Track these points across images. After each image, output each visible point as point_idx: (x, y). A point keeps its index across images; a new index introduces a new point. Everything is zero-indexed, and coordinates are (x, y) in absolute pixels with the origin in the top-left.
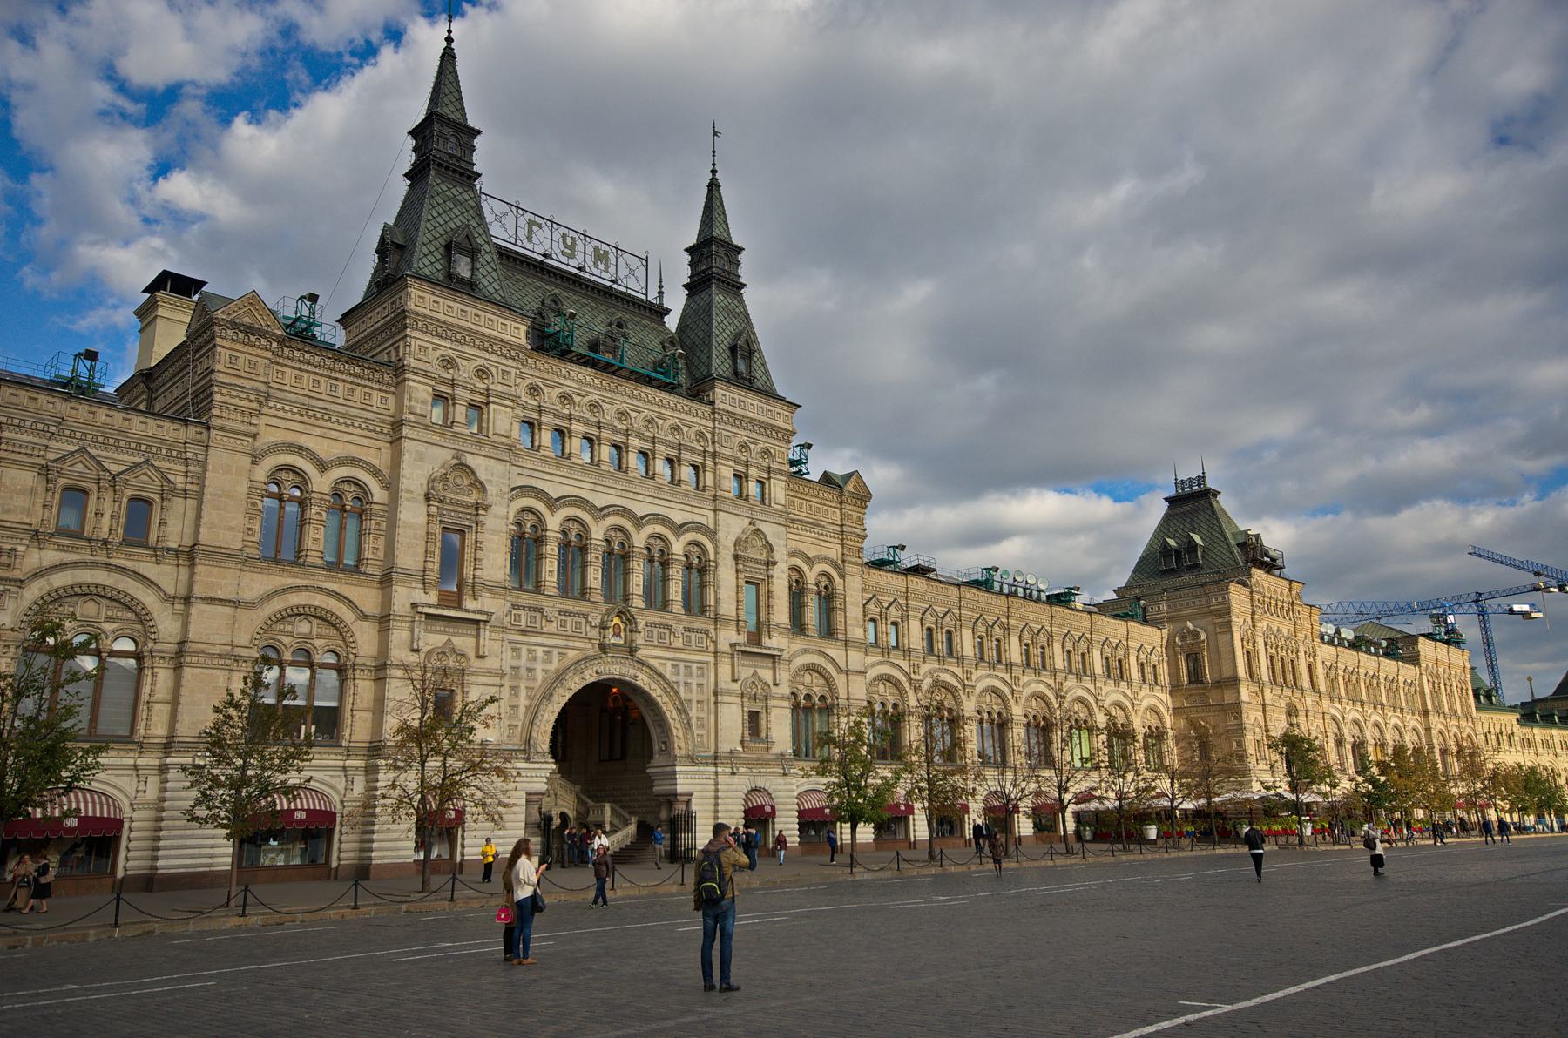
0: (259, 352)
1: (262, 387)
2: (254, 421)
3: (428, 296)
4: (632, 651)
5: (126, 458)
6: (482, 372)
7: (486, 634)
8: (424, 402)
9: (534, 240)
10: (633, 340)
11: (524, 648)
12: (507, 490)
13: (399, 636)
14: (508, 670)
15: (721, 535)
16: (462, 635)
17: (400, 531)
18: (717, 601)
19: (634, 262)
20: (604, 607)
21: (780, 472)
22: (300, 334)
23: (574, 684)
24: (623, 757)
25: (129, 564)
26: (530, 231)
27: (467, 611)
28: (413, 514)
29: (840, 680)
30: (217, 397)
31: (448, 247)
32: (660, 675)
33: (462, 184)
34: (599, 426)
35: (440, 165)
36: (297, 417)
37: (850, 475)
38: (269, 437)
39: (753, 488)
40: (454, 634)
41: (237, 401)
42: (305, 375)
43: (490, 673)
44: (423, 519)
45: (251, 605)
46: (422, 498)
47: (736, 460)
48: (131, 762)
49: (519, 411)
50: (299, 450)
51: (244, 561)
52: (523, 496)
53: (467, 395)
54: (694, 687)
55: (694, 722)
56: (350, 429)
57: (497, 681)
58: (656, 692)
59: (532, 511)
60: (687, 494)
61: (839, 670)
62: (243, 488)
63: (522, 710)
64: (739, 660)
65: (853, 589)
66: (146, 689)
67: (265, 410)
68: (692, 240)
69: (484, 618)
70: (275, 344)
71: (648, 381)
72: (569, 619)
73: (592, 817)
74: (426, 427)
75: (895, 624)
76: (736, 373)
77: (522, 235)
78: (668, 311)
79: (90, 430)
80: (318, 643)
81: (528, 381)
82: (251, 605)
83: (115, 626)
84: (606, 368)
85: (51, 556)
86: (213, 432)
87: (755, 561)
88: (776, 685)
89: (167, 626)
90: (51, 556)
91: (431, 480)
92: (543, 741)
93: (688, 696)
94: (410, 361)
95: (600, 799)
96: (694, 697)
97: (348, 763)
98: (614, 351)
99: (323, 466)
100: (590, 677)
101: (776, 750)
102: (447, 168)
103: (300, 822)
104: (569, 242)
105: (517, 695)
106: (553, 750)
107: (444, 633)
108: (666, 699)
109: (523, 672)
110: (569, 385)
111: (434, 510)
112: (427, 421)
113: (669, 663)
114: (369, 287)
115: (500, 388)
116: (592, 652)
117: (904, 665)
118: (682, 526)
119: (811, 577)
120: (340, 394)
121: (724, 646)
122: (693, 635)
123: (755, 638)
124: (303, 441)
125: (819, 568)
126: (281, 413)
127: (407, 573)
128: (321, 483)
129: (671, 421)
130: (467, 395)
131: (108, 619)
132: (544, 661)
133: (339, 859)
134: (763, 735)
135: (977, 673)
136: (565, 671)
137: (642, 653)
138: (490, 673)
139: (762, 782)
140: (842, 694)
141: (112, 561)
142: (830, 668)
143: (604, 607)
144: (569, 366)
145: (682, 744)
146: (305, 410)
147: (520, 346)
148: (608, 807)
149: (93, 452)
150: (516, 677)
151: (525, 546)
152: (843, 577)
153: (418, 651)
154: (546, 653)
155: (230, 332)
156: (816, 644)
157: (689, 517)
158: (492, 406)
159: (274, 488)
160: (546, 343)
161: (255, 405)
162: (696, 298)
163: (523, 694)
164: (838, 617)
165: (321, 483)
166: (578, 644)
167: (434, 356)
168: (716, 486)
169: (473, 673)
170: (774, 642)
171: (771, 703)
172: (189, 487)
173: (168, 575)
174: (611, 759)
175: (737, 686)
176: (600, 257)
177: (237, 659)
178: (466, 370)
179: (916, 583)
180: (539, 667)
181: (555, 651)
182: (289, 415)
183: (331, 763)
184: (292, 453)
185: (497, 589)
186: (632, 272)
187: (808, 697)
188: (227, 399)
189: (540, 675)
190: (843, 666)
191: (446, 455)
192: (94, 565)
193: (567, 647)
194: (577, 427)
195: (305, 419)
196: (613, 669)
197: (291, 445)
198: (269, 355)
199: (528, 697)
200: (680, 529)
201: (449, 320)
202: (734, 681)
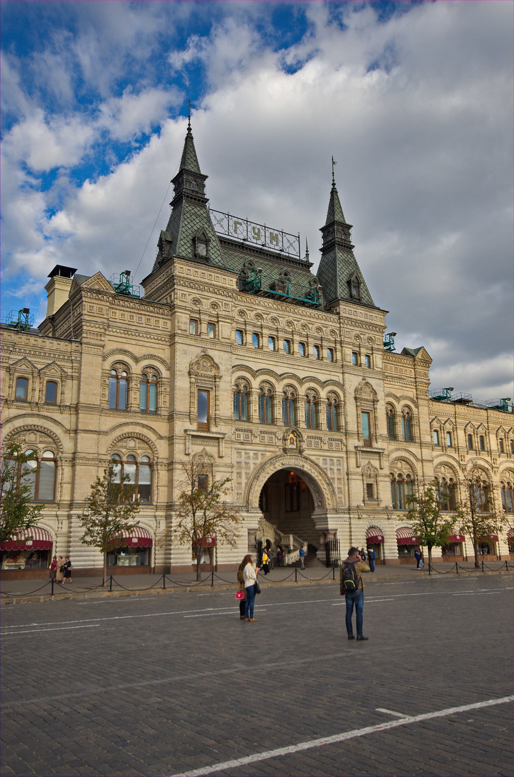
0: (103, 303)
1: (106, 321)
2: (103, 339)
3: (184, 267)
4: (301, 452)
5: (44, 361)
6: (214, 305)
7: (223, 445)
8: (185, 323)
9: (238, 232)
10: (294, 282)
11: (243, 452)
12: (230, 367)
13: (179, 447)
14: (235, 464)
15: (347, 386)
16: (211, 446)
17: (176, 392)
18: (346, 423)
19: (292, 239)
20: (285, 429)
21: (378, 350)
22: (122, 292)
23: (271, 471)
24: (299, 509)
25: (49, 414)
26: (236, 227)
27: (213, 433)
28: (183, 383)
29: (418, 466)
30: (85, 328)
31: (194, 240)
32: (317, 465)
33: (199, 206)
34: (277, 330)
35: (187, 197)
36: (123, 335)
37: (419, 349)
38: (110, 346)
39: (363, 360)
40: (206, 445)
41: (94, 329)
42: (126, 313)
43: (226, 465)
44: (188, 385)
45: (106, 433)
46: (187, 374)
47: (353, 345)
48: (55, 513)
49: (234, 325)
50: (125, 352)
51: (101, 410)
52: (239, 370)
53: (207, 318)
54: (335, 471)
55: (336, 490)
56: (149, 340)
57: (230, 470)
58: (314, 474)
59: (244, 378)
60: (327, 365)
61: (417, 459)
62: (99, 374)
63: (243, 485)
64: (360, 456)
65: (423, 413)
66: (59, 477)
67: (107, 333)
68: (323, 224)
69: (221, 436)
70: (111, 299)
71: (303, 304)
72: (266, 436)
73: (283, 542)
74: (187, 336)
75: (449, 433)
76: (351, 296)
77: (232, 229)
78: (312, 264)
79: (28, 348)
80: (139, 451)
81: (238, 309)
82: (106, 433)
83: (43, 445)
84: (280, 298)
85: (14, 412)
86: (84, 346)
87: (367, 400)
88: (381, 469)
89: (67, 444)
90: (14, 412)
91: (191, 365)
92: (255, 501)
93: (333, 476)
94: (177, 302)
95: (287, 532)
96: (336, 476)
97: (157, 514)
98: (283, 288)
99: (137, 360)
100: (279, 466)
101: (383, 505)
102: (191, 198)
103: (135, 544)
104: (257, 231)
105: (240, 477)
106: (261, 506)
107: (201, 445)
108: (320, 478)
109: (243, 464)
110: (260, 309)
111: (193, 380)
112: (188, 333)
113: (321, 458)
114: (155, 265)
115: (224, 313)
116: (279, 453)
117: (456, 456)
118: (325, 382)
119: (399, 407)
120: (143, 322)
121: (351, 448)
122: (334, 442)
123: (369, 443)
124: (127, 347)
125: (403, 402)
126: (115, 334)
127: (181, 414)
128: (137, 369)
129: (316, 325)
130: (207, 318)
131: (41, 442)
132: (254, 459)
133: (155, 563)
134: (375, 497)
135: (500, 460)
136: (265, 464)
137: (306, 453)
138: (226, 465)
139: (375, 523)
140: (420, 473)
141: (41, 413)
142: (412, 459)
143: (285, 429)
144: (260, 299)
145: (330, 503)
146: (127, 331)
147: (233, 290)
148: (291, 537)
149: (29, 359)
150: (240, 467)
151: (241, 397)
152: (417, 407)
153: (188, 455)
154: (255, 454)
155: (89, 294)
156: (404, 445)
157: (328, 378)
158: (220, 323)
159: (114, 373)
160: (248, 287)
161: (103, 331)
162: (327, 256)
163: (244, 476)
164: (416, 430)
165: (137, 369)
166: (271, 449)
167: (189, 299)
168: (343, 360)
169: (217, 466)
170: (379, 445)
171: (379, 479)
172: (74, 374)
173: (66, 419)
174: (292, 510)
175: (359, 470)
176: (274, 238)
177: (100, 461)
178: (206, 305)
179: (460, 409)
180: (251, 462)
181: (260, 453)
182: (119, 335)
183: (149, 514)
184: (122, 354)
185: (227, 421)
186: (291, 245)
187: (400, 475)
188: (89, 328)
189: (252, 466)
190: (419, 457)
191: (198, 351)
192: (33, 415)
193: (265, 451)
194: (265, 331)
195: (127, 336)
196: (291, 462)
197: (121, 350)
198: (108, 304)
199: (247, 478)
200: (324, 384)
201: (196, 279)
202: (358, 467)
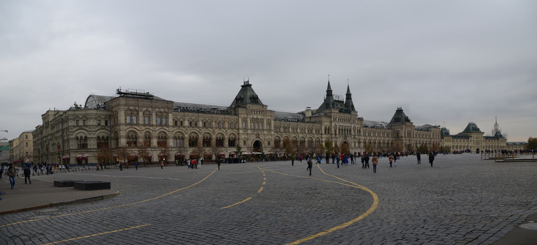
28: (333, 129)
170: (356, 137)
